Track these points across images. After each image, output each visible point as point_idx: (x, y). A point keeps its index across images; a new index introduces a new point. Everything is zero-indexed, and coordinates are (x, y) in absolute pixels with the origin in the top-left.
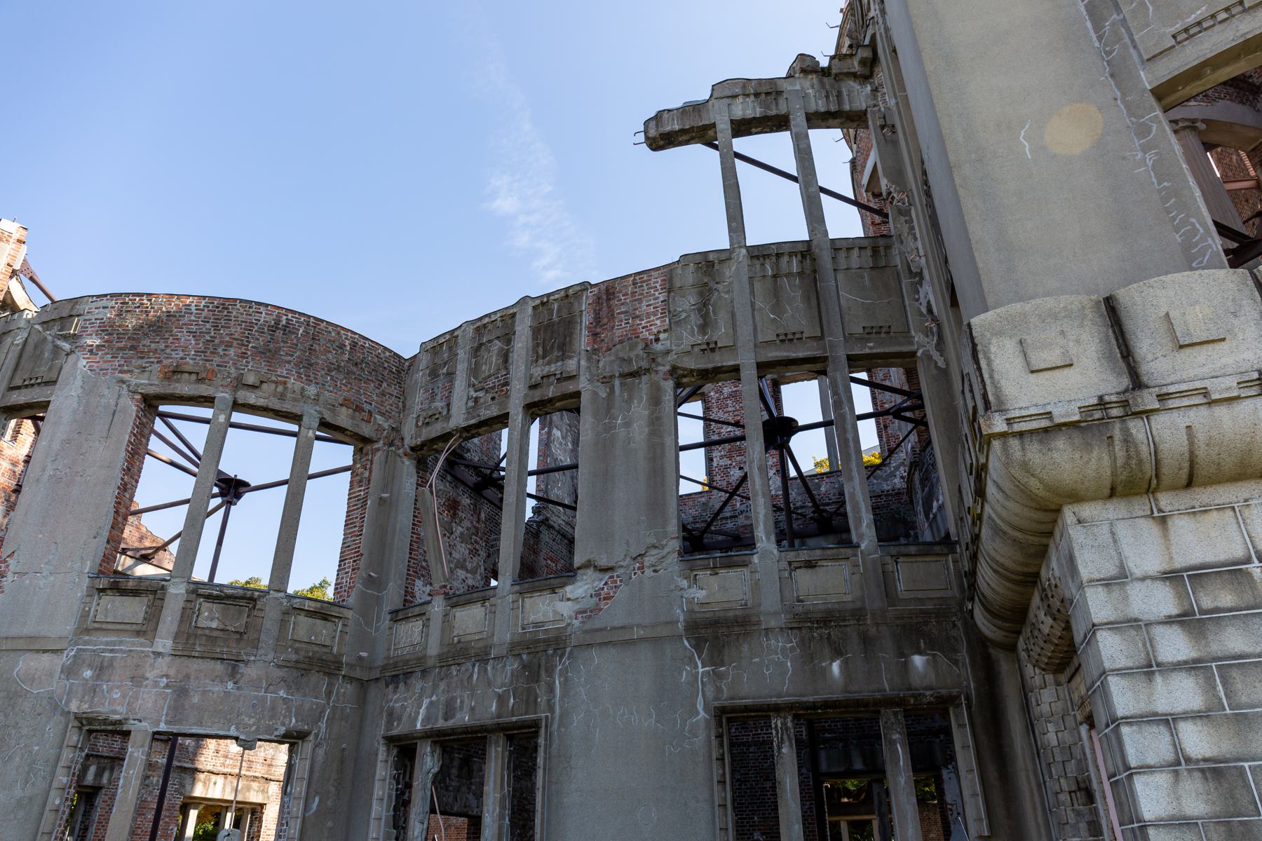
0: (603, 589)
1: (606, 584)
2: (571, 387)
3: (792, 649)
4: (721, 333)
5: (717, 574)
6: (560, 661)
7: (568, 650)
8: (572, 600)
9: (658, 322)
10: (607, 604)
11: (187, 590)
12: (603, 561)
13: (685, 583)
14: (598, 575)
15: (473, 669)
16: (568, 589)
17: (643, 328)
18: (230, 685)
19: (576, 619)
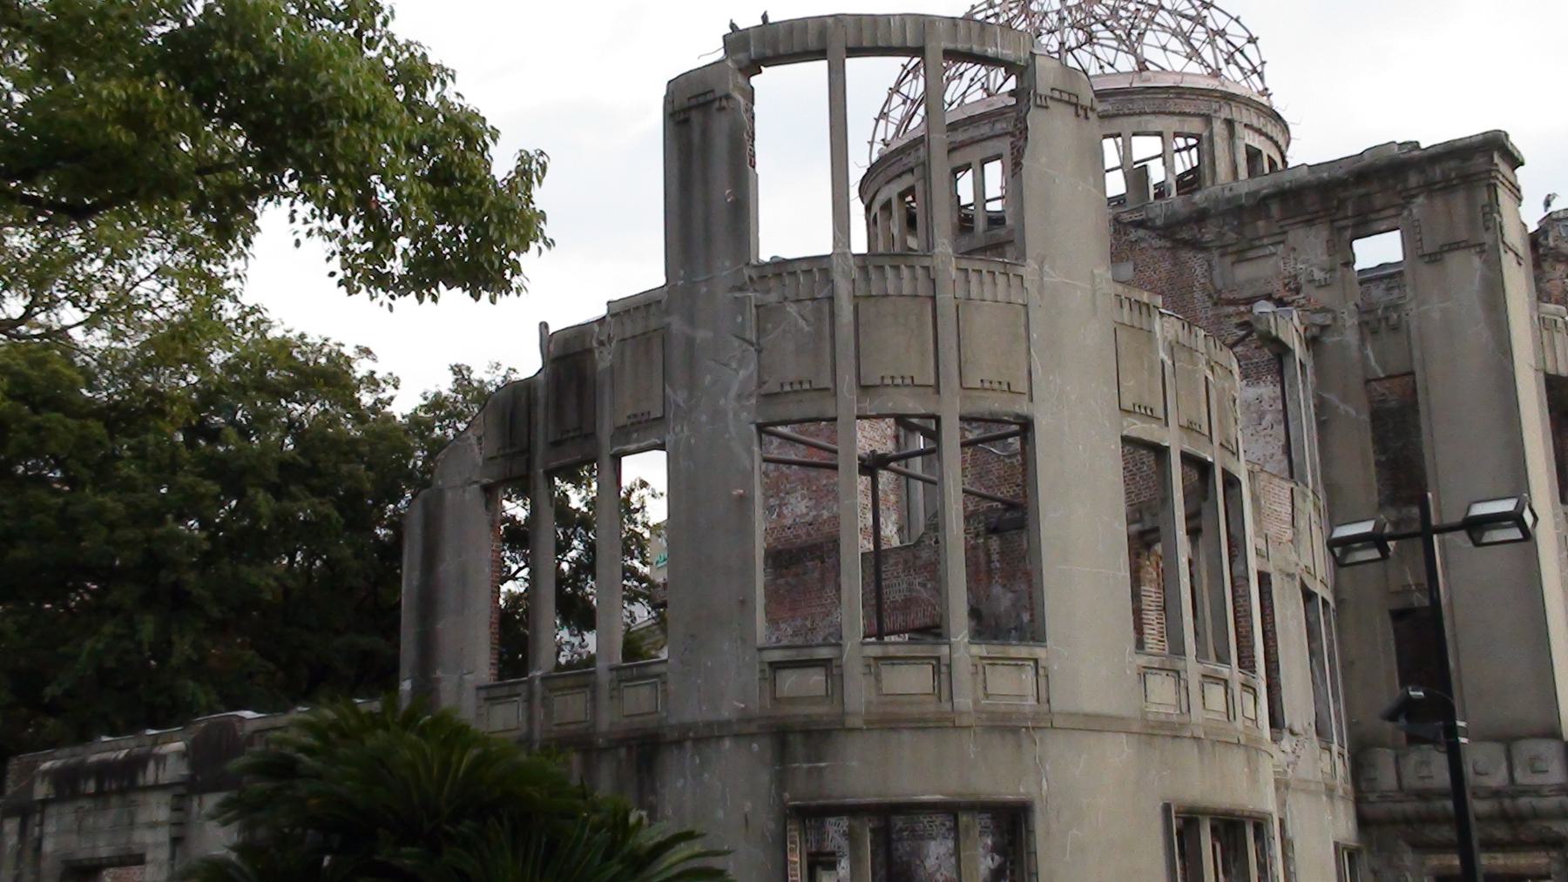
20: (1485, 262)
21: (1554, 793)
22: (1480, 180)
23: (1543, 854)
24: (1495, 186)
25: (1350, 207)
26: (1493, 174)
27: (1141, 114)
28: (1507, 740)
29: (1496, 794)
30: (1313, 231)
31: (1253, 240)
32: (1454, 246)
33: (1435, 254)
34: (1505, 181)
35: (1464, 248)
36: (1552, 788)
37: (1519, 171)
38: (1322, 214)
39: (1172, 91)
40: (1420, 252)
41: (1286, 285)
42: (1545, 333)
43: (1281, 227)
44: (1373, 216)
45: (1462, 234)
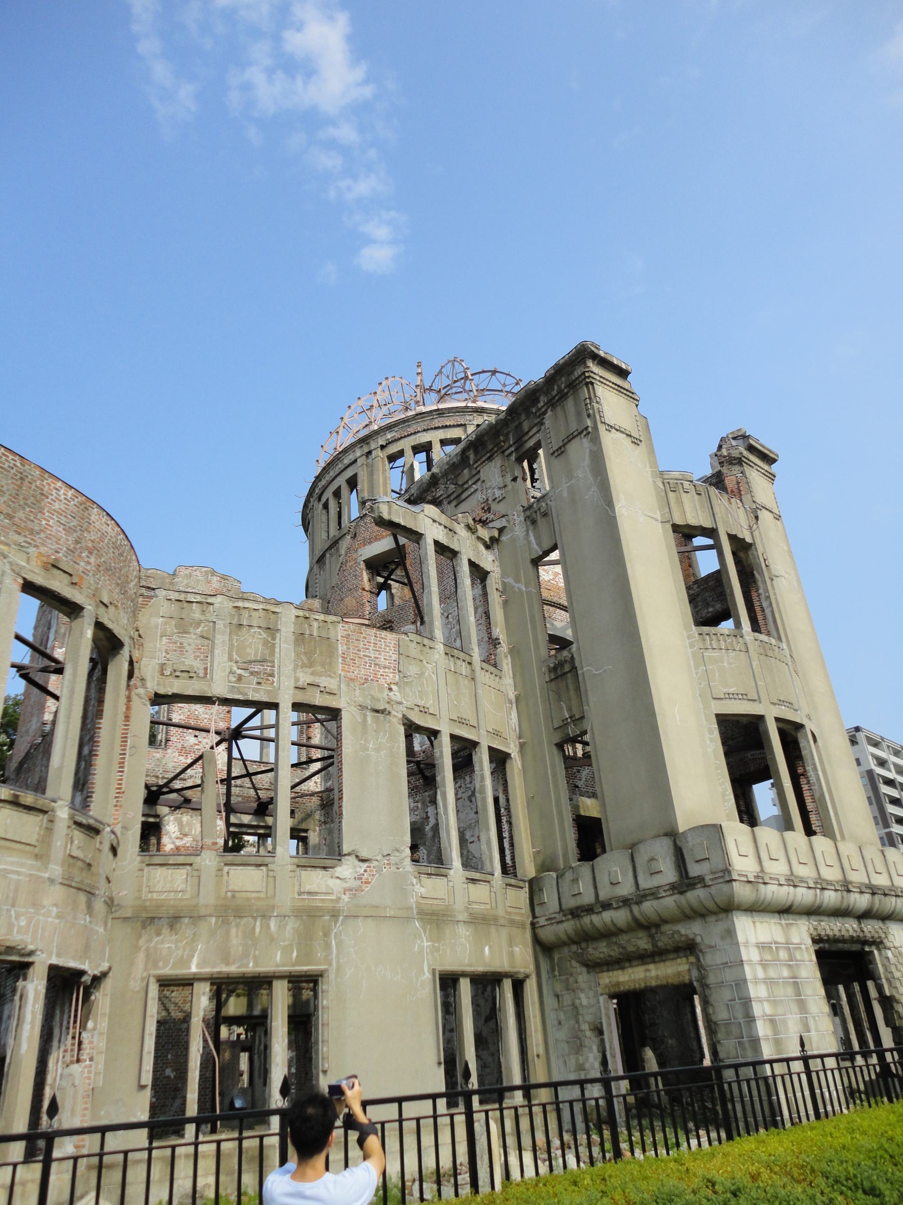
0: (363, 875)
1: (365, 871)
4: (430, 703)
6: (335, 926)
7: (341, 918)
9: (391, 675)
10: (367, 887)
11: (69, 815)
12: (364, 854)
13: (414, 881)
14: (357, 862)
15: (255, 923)
16: (338, 869)
17: (381, 675)
18: (88, 919)
19: (345, 894)
20: (592, 440)
21: (668, 893)
22: (581, 382)
23: (684, 959)
24: (592, 384)
25: (511, 439)
26: (587, 374)
27: (415, 433)
29: (626, 902)
30: (493, 463)
31: (463, 485)
32: (571, 438)
33: (560, 448)
34: (602, 380)
36: (667, 887)
38: (496, 449)
41: (483, 509)
42: (671, 495)
43: (476, 468)
44: (526, 438)
45: (574, 426)
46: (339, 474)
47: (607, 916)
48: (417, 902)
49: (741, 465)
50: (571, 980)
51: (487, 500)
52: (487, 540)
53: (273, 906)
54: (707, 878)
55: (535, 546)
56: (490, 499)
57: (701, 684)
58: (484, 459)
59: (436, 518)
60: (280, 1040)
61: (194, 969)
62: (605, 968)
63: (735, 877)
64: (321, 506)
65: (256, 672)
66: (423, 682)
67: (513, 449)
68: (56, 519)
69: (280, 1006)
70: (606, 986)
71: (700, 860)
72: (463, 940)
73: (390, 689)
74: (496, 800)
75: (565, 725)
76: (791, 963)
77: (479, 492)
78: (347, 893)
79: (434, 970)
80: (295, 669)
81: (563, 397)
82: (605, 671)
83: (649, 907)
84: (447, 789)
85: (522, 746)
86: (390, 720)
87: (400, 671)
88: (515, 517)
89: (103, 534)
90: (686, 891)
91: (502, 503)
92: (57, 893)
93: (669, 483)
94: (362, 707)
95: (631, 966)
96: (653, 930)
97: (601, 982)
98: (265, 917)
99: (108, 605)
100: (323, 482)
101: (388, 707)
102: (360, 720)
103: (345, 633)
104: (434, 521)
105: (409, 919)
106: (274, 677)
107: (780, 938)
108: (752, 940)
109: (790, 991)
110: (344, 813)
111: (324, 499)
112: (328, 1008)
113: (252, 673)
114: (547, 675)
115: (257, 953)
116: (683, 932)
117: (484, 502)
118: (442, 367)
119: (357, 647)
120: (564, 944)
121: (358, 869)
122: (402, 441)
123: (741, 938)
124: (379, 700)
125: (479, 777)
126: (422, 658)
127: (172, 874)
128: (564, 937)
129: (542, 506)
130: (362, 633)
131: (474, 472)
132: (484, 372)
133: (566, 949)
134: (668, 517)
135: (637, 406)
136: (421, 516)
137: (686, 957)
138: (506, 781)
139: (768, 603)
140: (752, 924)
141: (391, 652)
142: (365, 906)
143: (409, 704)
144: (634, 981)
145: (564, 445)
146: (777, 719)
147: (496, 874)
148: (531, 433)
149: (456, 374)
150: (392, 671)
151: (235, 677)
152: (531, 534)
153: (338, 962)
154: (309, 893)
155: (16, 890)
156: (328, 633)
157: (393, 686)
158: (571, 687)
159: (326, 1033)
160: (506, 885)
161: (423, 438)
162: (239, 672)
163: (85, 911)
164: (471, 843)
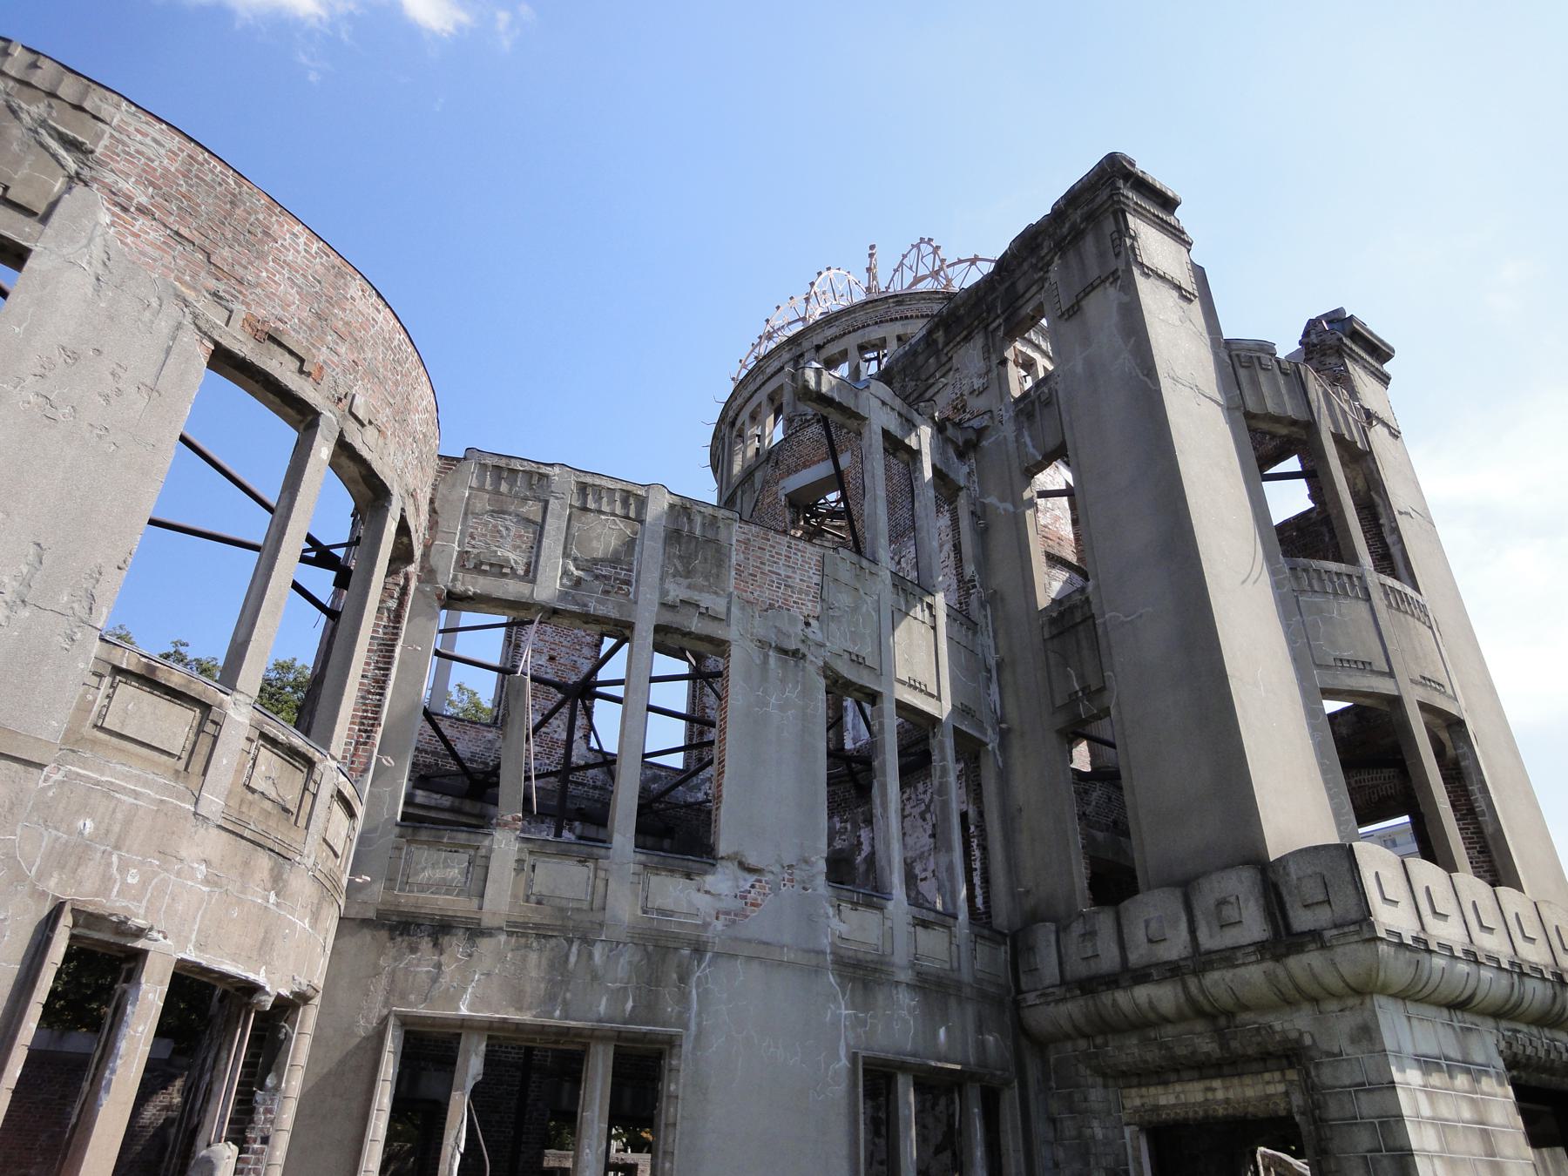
0: (750, 892)
1: (753, 886)
2: (718, 631)
3: (915, 1007)
5: (856, 910)
6: (699, 966)
7: (709, 955)
8: (712, 895)
9: (809, 604)
10: (754, 911)
12: (752, 861)
13: (831, 911)
14: (741, 874)
16: (709, 879)
17: (795, 602)
18: (272, 897)
21: (1253, 958)
22: (1106, 210)
23: (1277, 1075)
27: (864, 327)
28: (1186, 887)
29: (1173, 971)
32: (1090, 288)
33: (1073, 306)
35: (1098, 286)
36: (1252, 949)
37: (1177, 213)
38: (976, 323)
39: (891, 300)
40: (1059, 313)
43: (947, 354)
44: (1021, 302)
45: (1094, 273)
46: (759, 388)
47: (1142, 993)
48: (833, 944)
49: (1341, 357)
50: (1077, 1097)
51: (962, 395)
52: (961, 444)
53: (601, 925)
54: (1327, 934)
55: (1031, 450)
56: (966, 393)
57: (1296, 642)
58: (958, 339)
59: (887, 400)
60: (595, 1143)
61: (464, 1011)
62: (1135, 1081)
63: (1381, 934)
64: (735, 433)
65: (605, 576)
66: (858, 620)
67: (1000, 320)
68: (287, 275)
69: (599, 1085)
70: (1136, 1110)
71: (1313, 904)
72: (904, 1013)
73: (807, 624)
74: (964, 816)
75: (1073, 699)
76: (1475, 1096)
77: (950, 388)
78: (722, 917)
79: (855, 1055)
80: (662, 579)
81: (1077, 235)
82: (1141, 616)
83: (1218, 982)
84: (888, 779)
85: (1004, 735)
86: (804, 667)
87: (823, 600)
88: (1003, 412)
89: (367, 319)
90: (1287, 955)
91: (983, 397)
92: (214, 843)
93: (1238, 356)
94: (763, 644)
95: (1180, 1080)
96: (1222, 1021)
97: (1128, 1103)
98: (587, 942)
99: (366, 422)
100: (740, 401)
101: (803, 649)
102: (758, 662)
103: (743, 536)
104: (884, 403)
105: (817, 970)
106: (631, 586)
107: (1454, 1052)
108: (1408, 1048)
109: (1476, 1146)
110: (724, 796)
111: (738, 424)
112: (677, 1097)
113: (597, 577)
114: (1046, 629)
115: (568, 995)
116: (1278, 1026)
117: (957, 398)
118: (904, 256)
119: (760, 558)
120: (1068, 1037)
121: (741, 883)
122: (846, 338)
123: (1389, 1044)
124: (789, 636)
125: (938, 768)
126: (858, 586)
127: (446, 859)
128: (1067, 1027)
129: (1043, 392)
130: (769, 540)
131: (944, 359)
132: (960, 261)
133: (1069, 1046)
134: (1237, 400)
135: (1189, 251)
136: (865, 394)
137: (1282, 1071)
138: (979, 785)
139: (1395, 537)
140: (1405, 1020)
141: (811, 572)
142: (749, 941)
143: (836, 649)
144: (1185, 1104)
145: (1078, 302)
146: (1424, 707)
147: (960, 918)
148: (1028, 295)
149: (923, 257)
150: (811, 598)
151: (570, 580)
152: (1026, 433)
153: (699, 1024)
154: (662, 912)
155: (128, 822)
156: (717, 533)
157: (811, 621)
158: (1084, 643)
159: (670, 1140)
160: (976, 936)
161: (875, 333)
162: (576, 573)
163: (269, 885)
164: (922, 880)
